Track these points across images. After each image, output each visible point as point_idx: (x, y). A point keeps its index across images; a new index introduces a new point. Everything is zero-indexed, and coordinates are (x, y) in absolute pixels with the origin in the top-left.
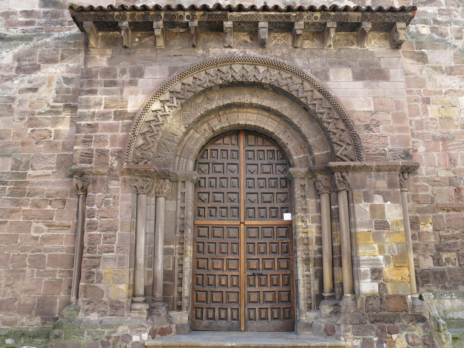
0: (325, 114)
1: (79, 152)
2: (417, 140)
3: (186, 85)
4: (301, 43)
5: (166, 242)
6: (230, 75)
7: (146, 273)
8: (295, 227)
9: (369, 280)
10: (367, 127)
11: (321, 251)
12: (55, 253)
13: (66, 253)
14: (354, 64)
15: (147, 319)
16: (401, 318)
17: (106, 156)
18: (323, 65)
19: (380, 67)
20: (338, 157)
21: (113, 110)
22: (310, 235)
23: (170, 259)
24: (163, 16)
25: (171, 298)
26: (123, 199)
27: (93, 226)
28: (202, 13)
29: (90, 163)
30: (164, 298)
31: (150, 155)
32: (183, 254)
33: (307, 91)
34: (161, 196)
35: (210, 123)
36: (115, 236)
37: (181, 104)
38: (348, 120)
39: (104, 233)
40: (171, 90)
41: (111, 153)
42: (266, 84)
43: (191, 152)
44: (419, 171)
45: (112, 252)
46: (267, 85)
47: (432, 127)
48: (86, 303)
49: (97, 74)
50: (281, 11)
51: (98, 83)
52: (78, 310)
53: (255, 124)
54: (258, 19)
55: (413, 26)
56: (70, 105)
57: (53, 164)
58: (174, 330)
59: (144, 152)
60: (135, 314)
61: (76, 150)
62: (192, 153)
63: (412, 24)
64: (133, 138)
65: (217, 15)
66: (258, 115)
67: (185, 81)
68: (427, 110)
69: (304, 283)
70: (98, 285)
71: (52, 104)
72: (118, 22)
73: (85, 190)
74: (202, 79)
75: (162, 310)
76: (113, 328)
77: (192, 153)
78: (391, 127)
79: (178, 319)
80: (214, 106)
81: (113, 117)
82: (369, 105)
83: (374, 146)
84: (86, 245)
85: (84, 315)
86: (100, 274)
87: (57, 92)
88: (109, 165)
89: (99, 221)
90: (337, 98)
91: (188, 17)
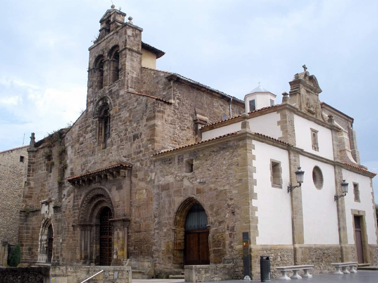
5: (91, 244)
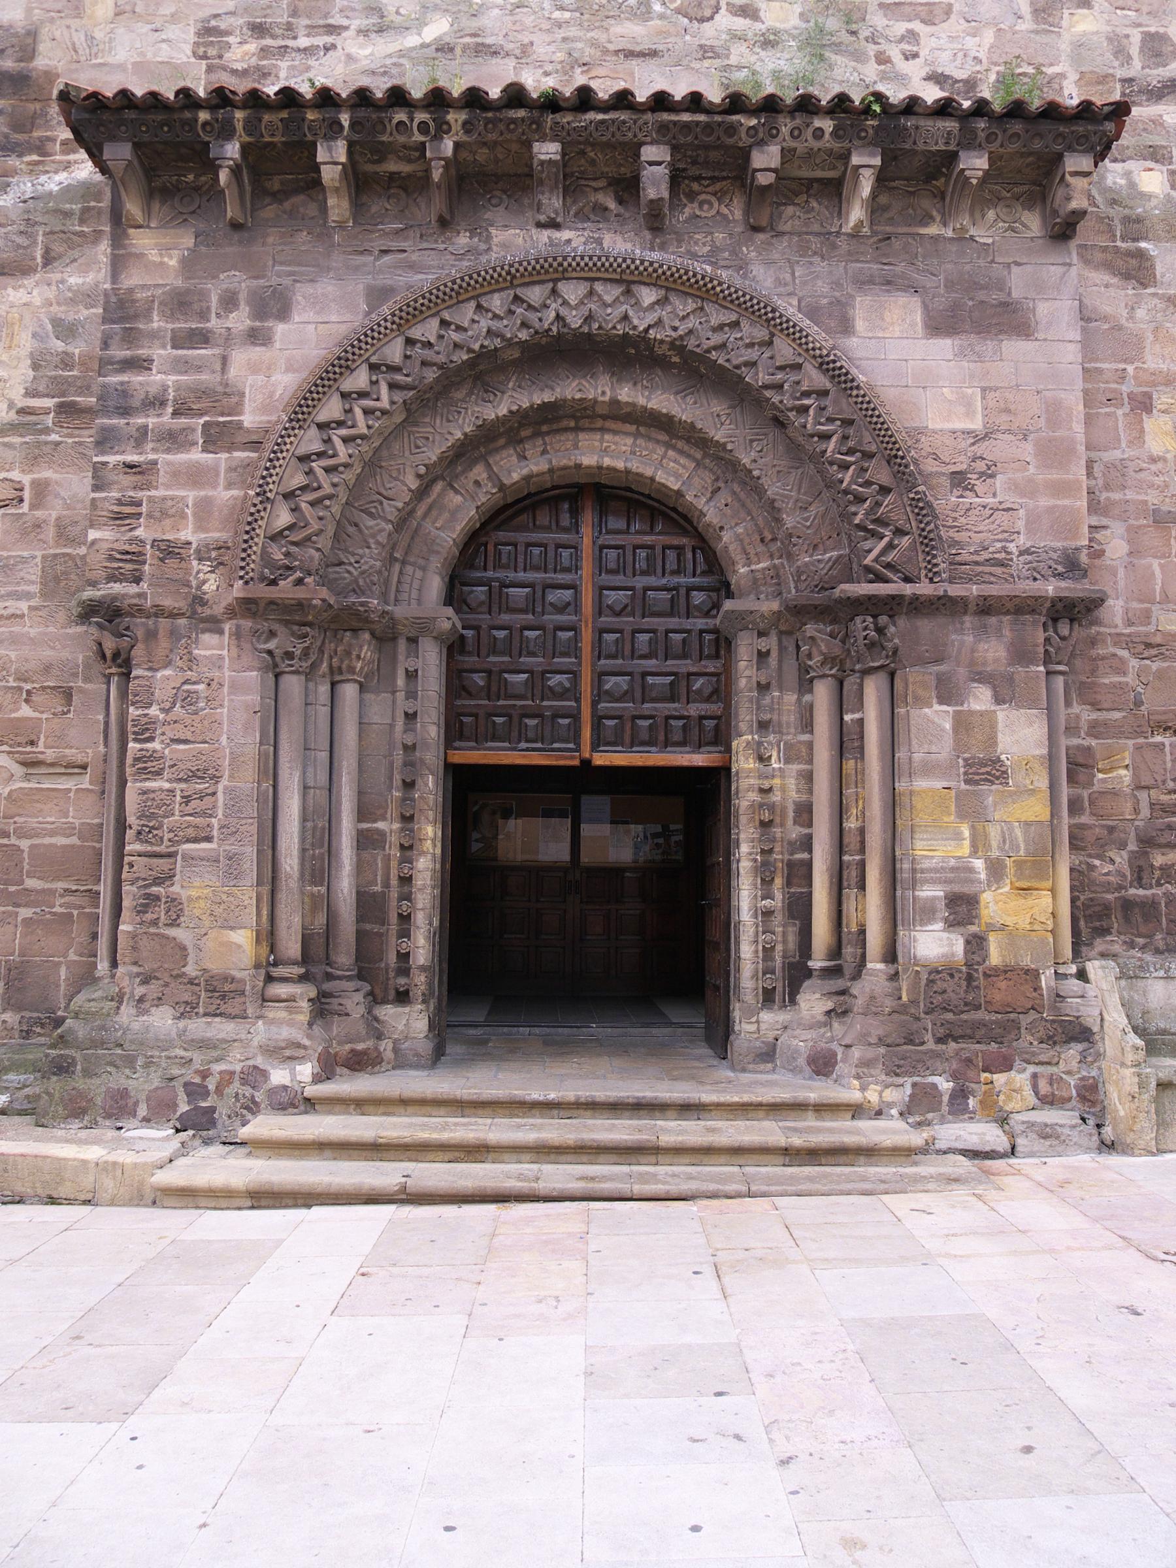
0: (834, 439)
1: (106, 546)
2: (1105, 521)
3: (419, 345)
4: (772, 214)
5: (363, 813)
6: (553, 314)
7: (306, 900)
8: (737, 773)
9: (939, 925)
10: (959, 480)
11: (807, 844)
12: (47, 841)
13: (78, 843)
14: (929, 282)
15: (310, 1024)
16: (1023, 1031)
17: (182, 559)
18: (837, 285)
19: (1009, 294)
20: (868, 569)
21: (202, 421)
22: (776, 797)
23: (376, 860)
24: (346, 124)
25: (379, 968)
26: (235, 687)
27: (149, 766)
28: (463, 116)
29: (137, 580)
30: (360, 970)
31: (312, 558)
32: (411, 847)
33: (781, 368)
34: (348, 681)
35: (491, 461)
36: (214, 794)
37: (404, 401)
38: (902, 458)
39: (183, 786)
40: (374, 360)
41: (198, 551)
42: (662, 342)
43: (436, 548)
44: (1103, 613)
45: (208, 839)
46: (665, 347)
47: (1152, 486)
48: (138, 980)
49: (149, 310)
50: (709, 109)
51: (154, 335)
52: (119, 998)
53: (629, 465)
54: (640, 136)
55: (1118, 167)
56: (73, 404)
57: (33, 583)
58: (389, 1054)
59: (294, 549)
60: (277, 1012)
61: (94, 542)
62: (438, 552)
63: (1115, 160)
64: (260, 507)
65: (513, 121)
66: (636, 439)
67: (416, 333)
68: (1142, 431)
69: (757, 932)
70: (172, 932)
71: (21, 402)
72: (208, 143)
73: (122, 663)
74: (466, 325)
75: (354, 1002)
76: (215, 1047)
77: (438, 552)
78: (1030, 480)
79: (401, 1027)
80: (503, 411)
81: (201, 441)
82: (970, 413)
83: (977, 538)
84: (131, 819)
85: (133, 1011)
86: (174, 900)
87: (35, 366)
88: (191, 587)
89: (167, 752)
90: (871, 387)
91: (423, 128)
